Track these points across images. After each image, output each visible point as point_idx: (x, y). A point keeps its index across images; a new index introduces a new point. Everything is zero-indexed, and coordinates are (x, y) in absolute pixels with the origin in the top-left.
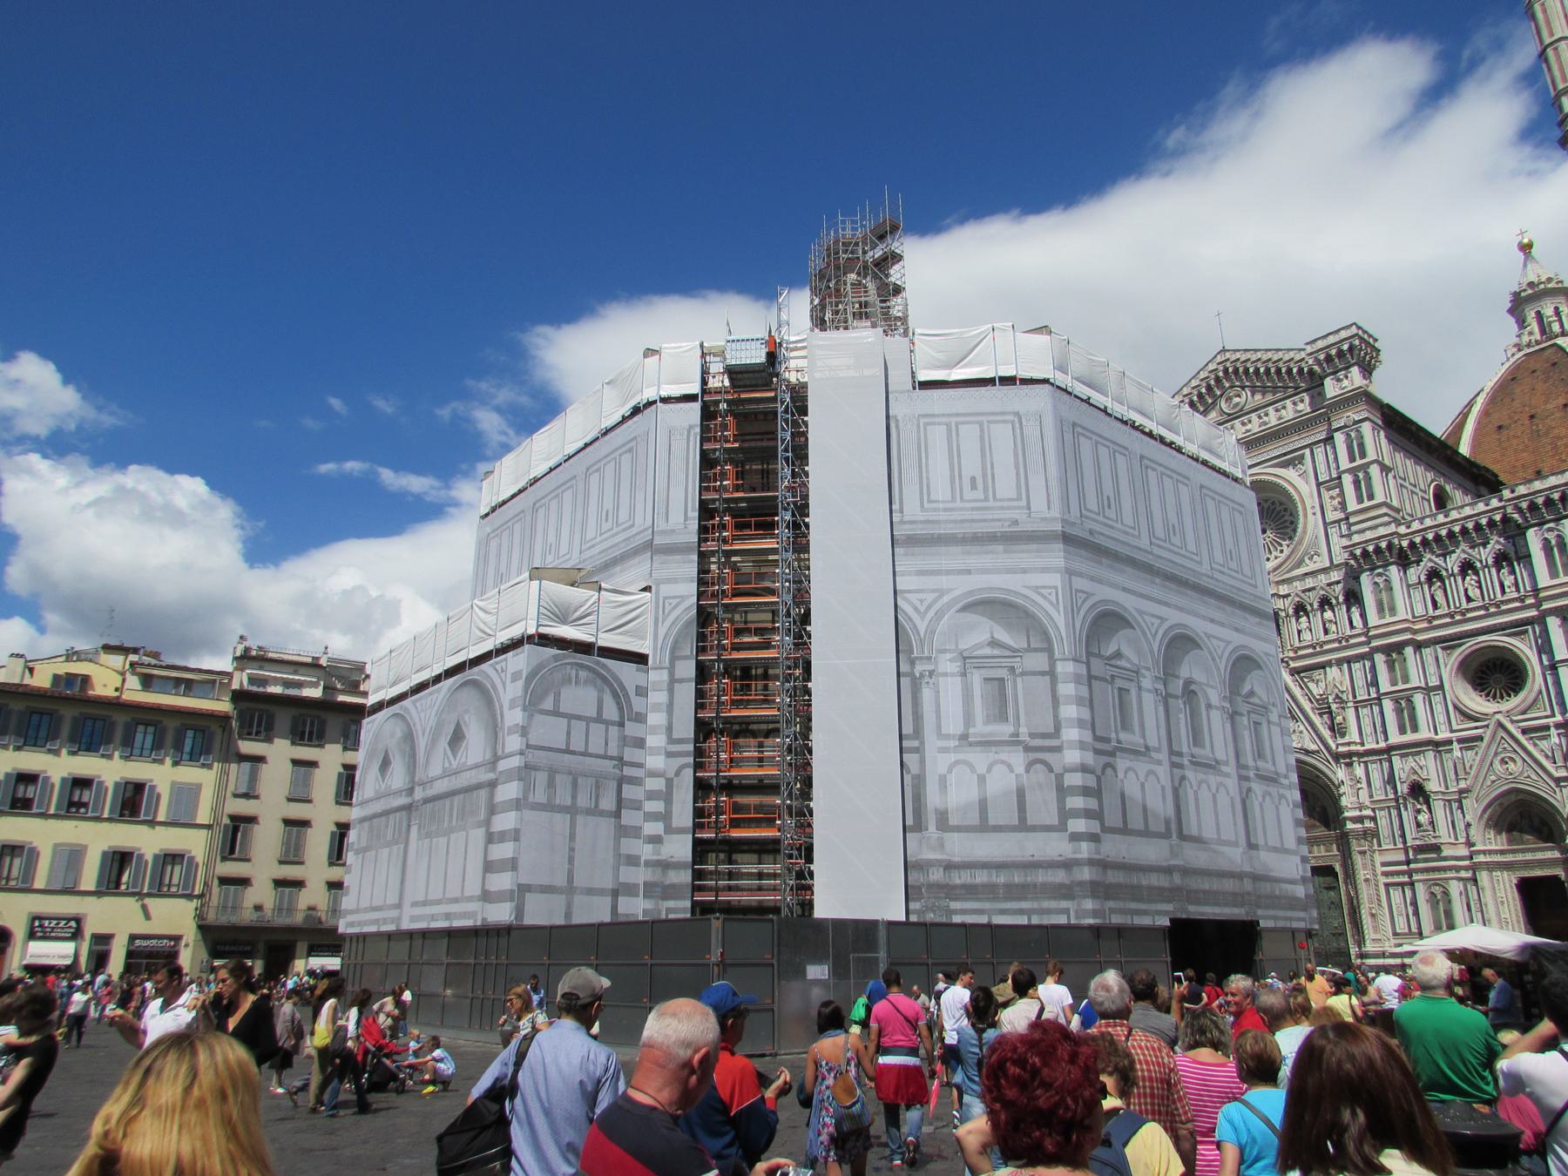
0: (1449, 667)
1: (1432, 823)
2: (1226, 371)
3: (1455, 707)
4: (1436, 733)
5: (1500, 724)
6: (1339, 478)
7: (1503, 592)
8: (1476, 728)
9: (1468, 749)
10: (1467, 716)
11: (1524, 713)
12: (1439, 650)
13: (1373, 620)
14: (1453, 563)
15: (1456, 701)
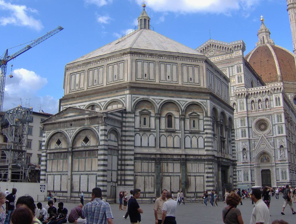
0: (254, 123)
1: (247, 158)
2: (210, 45)
3: (254, 132)
4: (249, 138)
5: (262, 136)
6: (235, 76)
7: (266, 108)
8: (258, 137)
9: (256, 141)
10: (255, 134)
11: (267, 134)
12: (252, 119)
13: (239, 111)
14: (257, 99)
15: (254, 131)
